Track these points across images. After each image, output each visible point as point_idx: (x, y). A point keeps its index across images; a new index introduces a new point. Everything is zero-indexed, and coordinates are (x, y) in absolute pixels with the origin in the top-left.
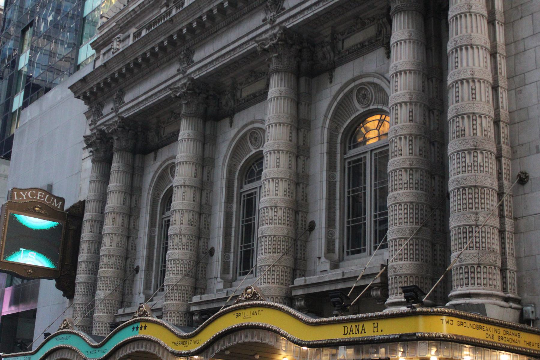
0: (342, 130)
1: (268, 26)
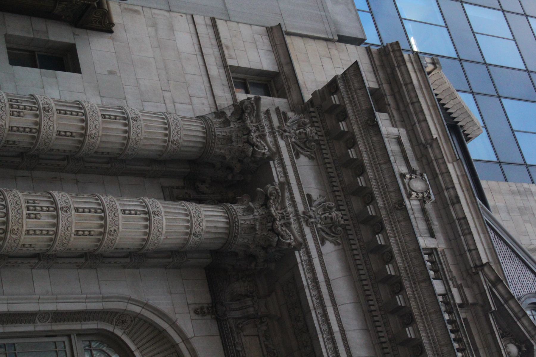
0: (118, 332)
1: (301, 208)
